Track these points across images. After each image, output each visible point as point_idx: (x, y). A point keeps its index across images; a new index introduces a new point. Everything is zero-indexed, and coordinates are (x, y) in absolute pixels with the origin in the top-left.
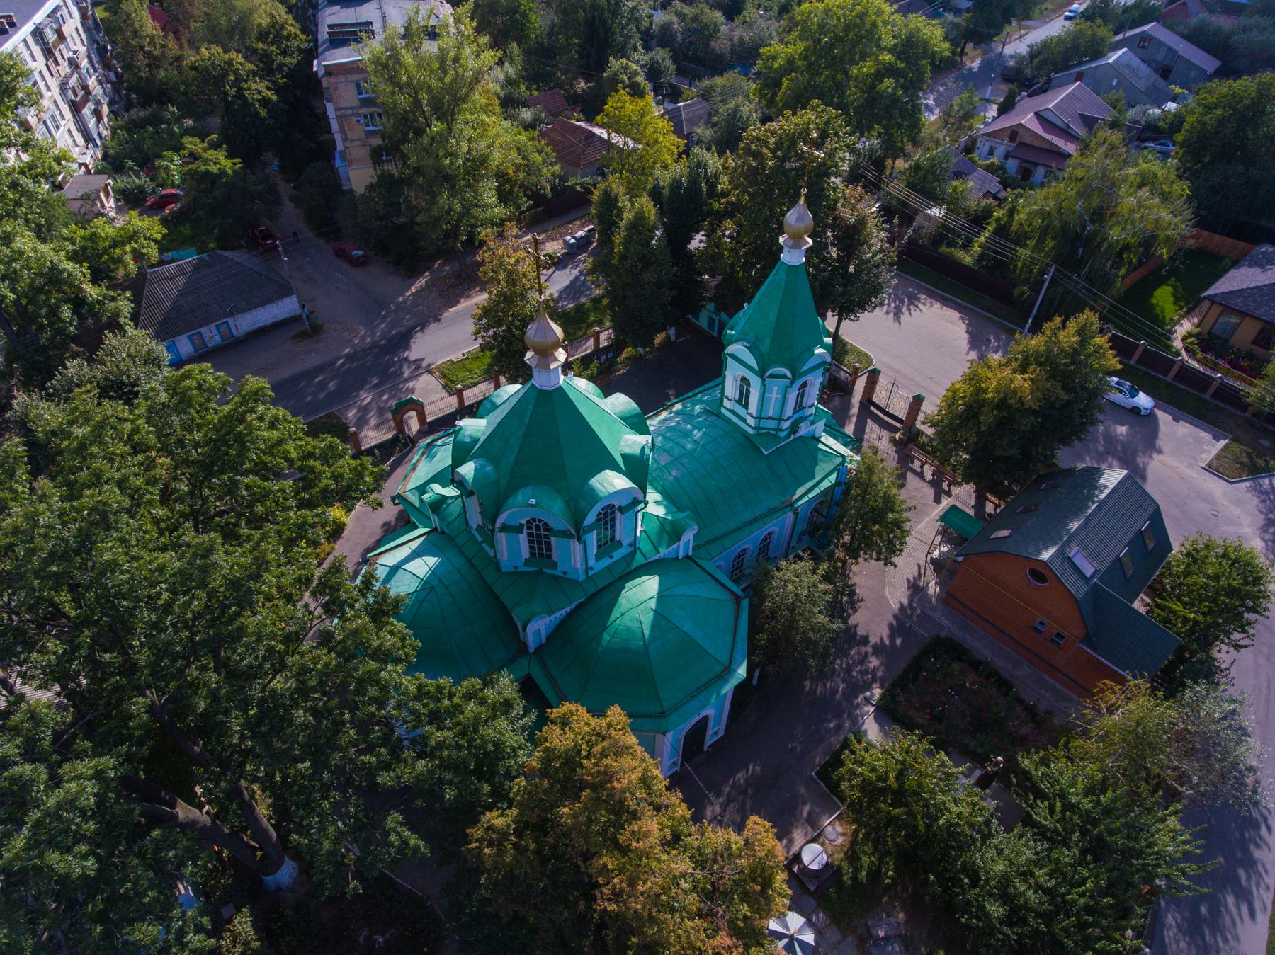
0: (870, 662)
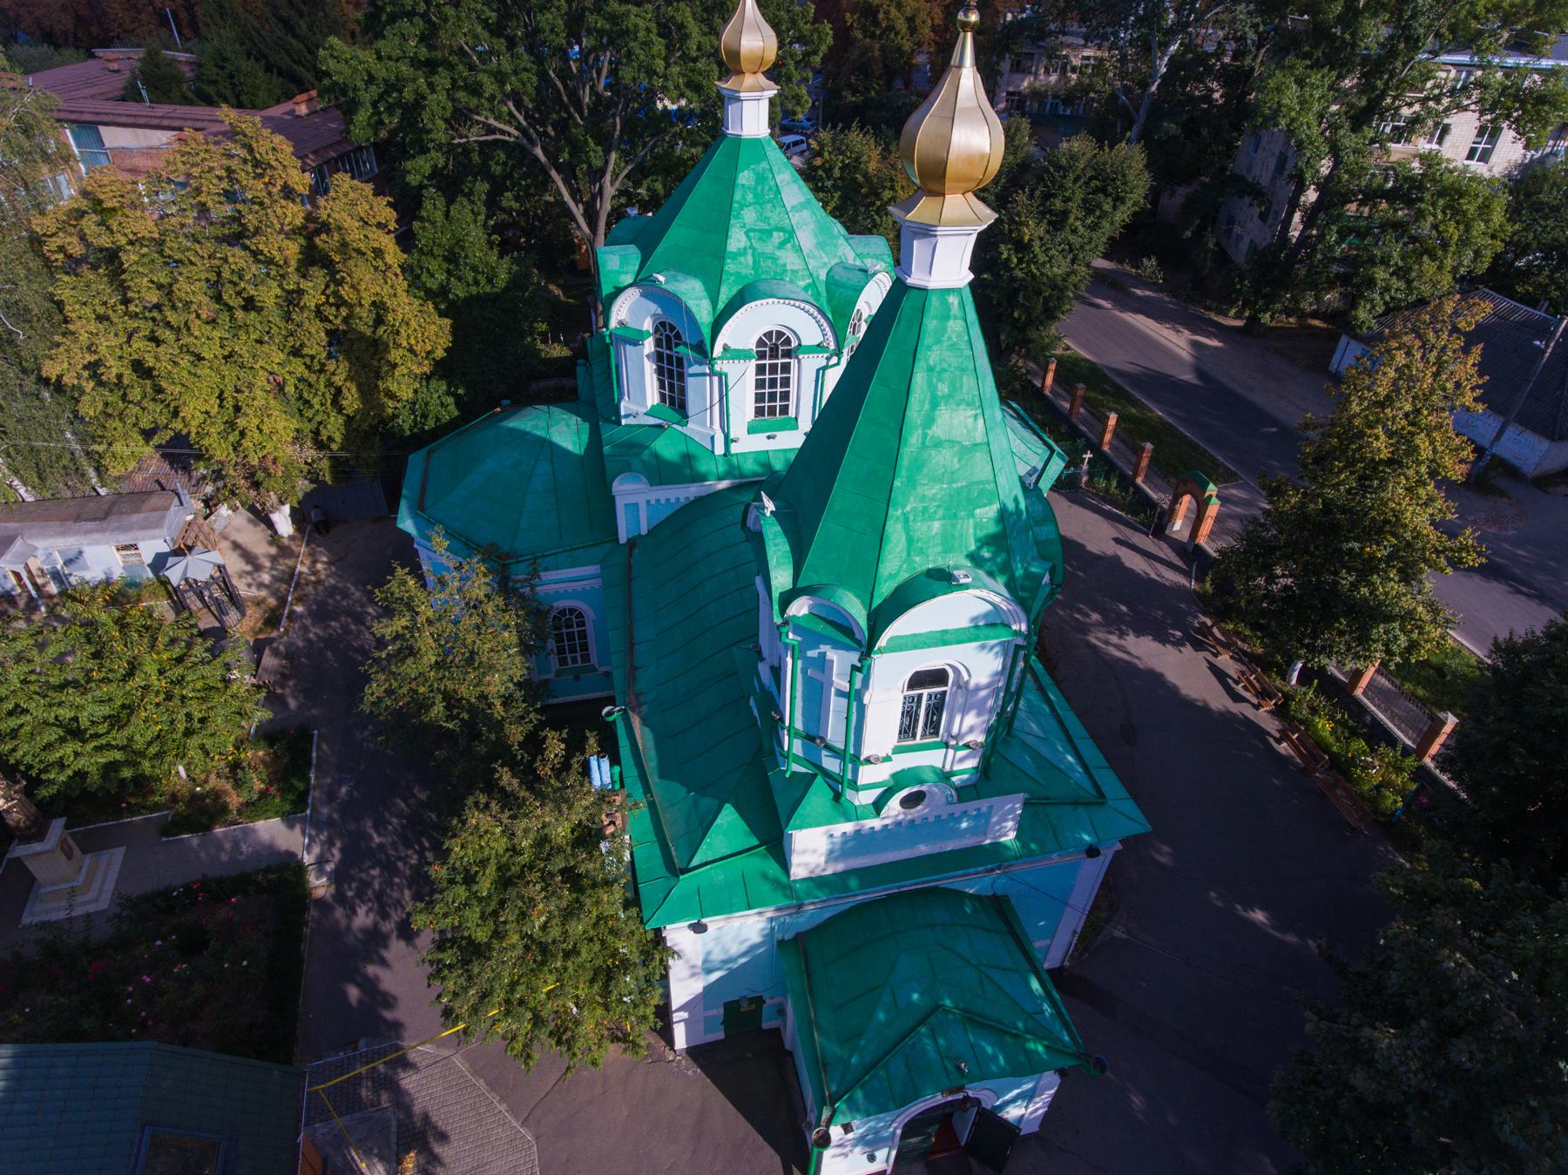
0: (370, 910)
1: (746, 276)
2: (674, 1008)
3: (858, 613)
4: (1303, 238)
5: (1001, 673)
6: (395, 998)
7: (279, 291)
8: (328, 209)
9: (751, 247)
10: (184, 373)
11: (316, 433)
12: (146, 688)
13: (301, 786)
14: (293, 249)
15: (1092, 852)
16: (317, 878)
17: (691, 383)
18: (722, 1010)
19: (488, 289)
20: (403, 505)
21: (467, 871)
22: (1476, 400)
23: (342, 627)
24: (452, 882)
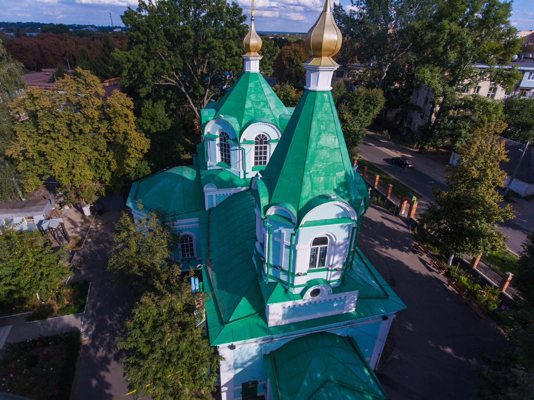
0: (104, 349)
1: (251, 116)
2: (222, 385)
3: (295, 213)
4: (436, 122)
5: (348, 238)
6: (111, 385)
7: (91, 128)
8: (109, 100)
9: (253, 107)
10: (56, 154)
11: (101, 178)
12: (27, 261)
13: (82, 302)
14: (96, 113)
15: (385, 318)
16: (85, 337)
17: (232, 153)
18: (241, 387)
19: (164, 129)
20: (129, 199)
21: (141, 322)
22: (506, 158)
23: (104, 246)
24: (134, 328)
